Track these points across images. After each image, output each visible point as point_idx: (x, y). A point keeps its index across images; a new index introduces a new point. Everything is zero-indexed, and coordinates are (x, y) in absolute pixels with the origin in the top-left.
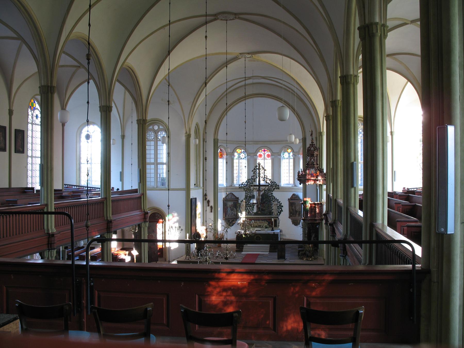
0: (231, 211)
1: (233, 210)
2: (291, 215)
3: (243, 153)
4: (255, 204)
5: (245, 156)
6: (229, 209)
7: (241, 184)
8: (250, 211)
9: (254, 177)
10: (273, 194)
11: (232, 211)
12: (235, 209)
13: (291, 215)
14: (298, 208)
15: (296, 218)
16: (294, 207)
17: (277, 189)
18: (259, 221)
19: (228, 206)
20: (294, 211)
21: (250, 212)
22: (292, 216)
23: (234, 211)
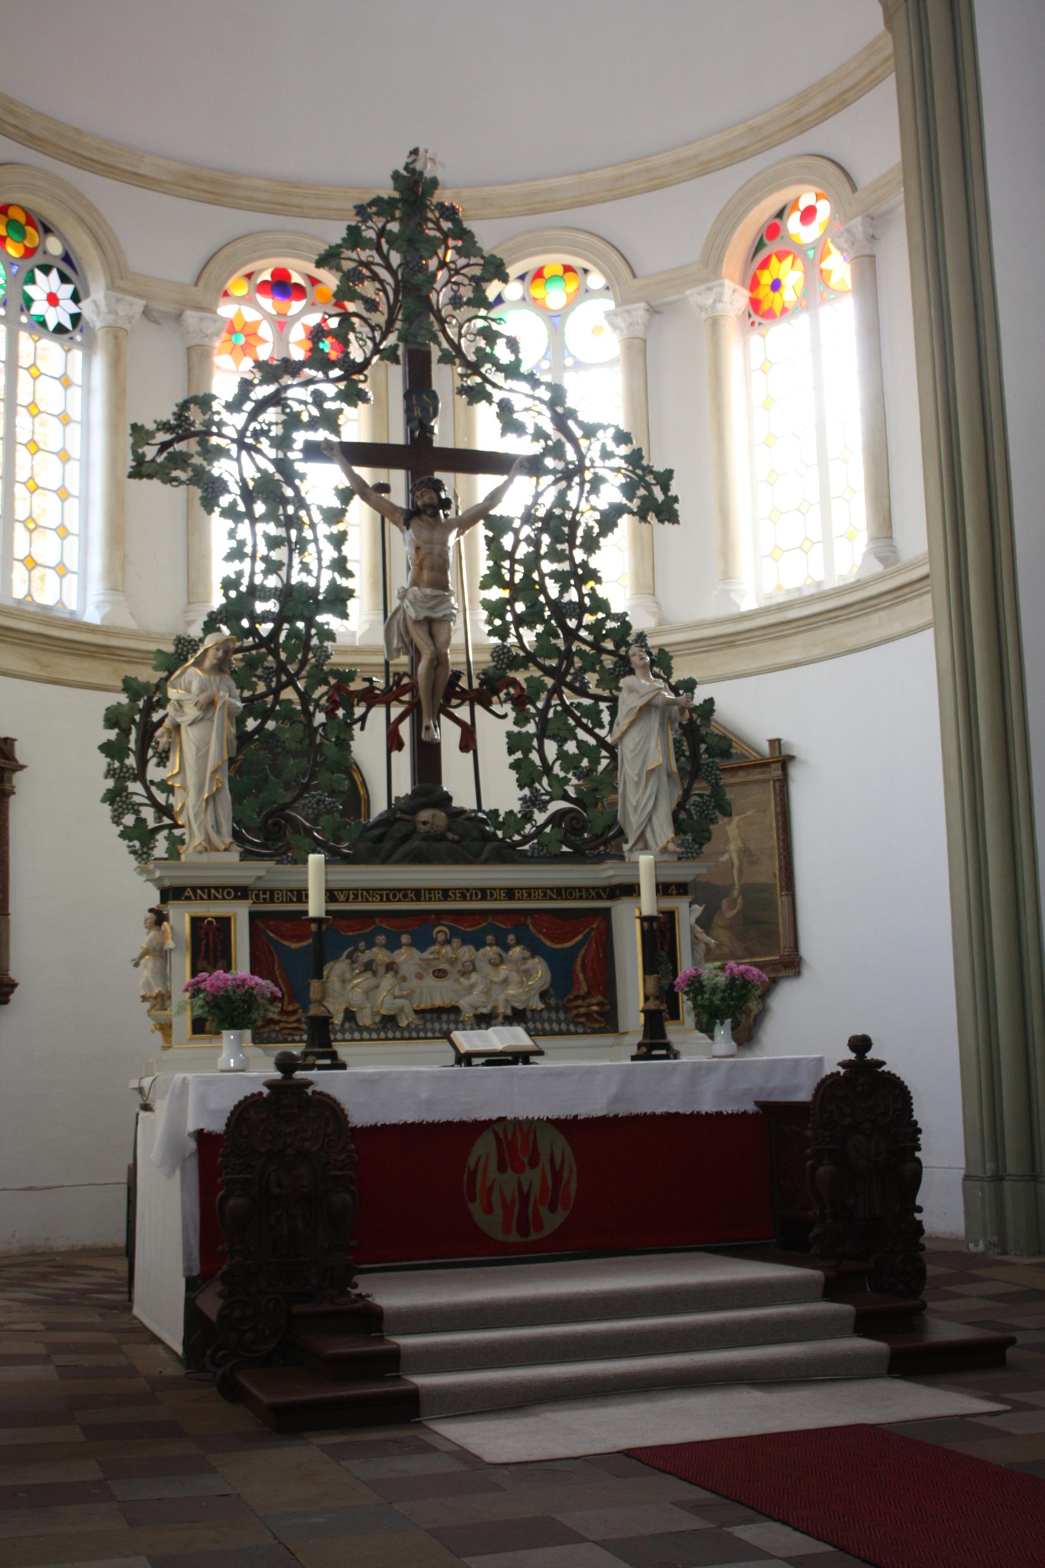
3: (54, 273)
4: (358, 711)
5: (74, 309)
7: (165, 427)
9: (346, 343)
10: (592, 575)
17: (643, 518)
18: (422, 943)
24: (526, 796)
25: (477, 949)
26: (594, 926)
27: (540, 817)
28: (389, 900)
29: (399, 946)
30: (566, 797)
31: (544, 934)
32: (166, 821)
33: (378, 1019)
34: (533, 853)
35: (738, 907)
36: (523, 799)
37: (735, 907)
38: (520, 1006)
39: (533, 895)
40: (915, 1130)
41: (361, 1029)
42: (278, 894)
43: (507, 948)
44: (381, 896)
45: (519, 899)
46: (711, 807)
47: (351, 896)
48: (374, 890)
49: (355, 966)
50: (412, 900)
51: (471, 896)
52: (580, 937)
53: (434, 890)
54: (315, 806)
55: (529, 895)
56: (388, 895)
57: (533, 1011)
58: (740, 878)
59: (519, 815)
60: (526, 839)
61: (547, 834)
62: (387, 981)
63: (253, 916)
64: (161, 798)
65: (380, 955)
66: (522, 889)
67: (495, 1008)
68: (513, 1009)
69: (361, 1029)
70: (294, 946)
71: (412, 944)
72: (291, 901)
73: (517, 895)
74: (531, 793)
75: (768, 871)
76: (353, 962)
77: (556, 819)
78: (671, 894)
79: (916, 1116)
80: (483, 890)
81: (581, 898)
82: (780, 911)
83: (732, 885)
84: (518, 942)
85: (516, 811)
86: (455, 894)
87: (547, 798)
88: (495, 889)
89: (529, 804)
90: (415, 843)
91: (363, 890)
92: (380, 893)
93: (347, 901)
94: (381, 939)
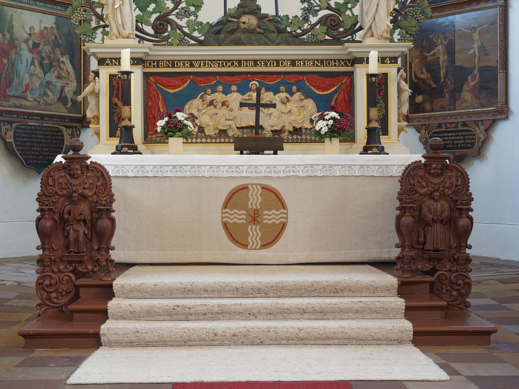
0: (38, 70)
1: (51, 66)
2: (419, 99)
6: (26, 55)
8: (169, 14)
11: (46, 69)
12: (65, 59)
13: (419, 99)
14: (476, 46)
15: (462, 115)
16: (440, 48)
18: (243, 90)
19: (20, 33)
20: (442, 73)
21: (170, 22)
22: (428, 107)
23: (59, 77)
24: (305, 7)
25: (275, 95)
26: (344, 82)
27: (313, 20)
28: (223, 66)
29: (230, 92)
30: (329, 8)
31: (314, 86)
32: (102, 23)
33: (217, 131)
34: (308, 40)
35: (477, 80)
36: (303, 9)
37: (475, 80)
38: (298, 126)
39: (306, 63)
40: (470, 198)
41: (206, 137)
42: (161, 63)
43: (292, 94)
44: (219, 64)
45: (298, 66)
46: (418, 13)
47: (202, 64)
48: (215, 61)
49: (204, 102)
50: (236, 66)
51: (270, 64)
52: (335, 88)
53: (249, 60)
54: (183, 14)
55: (304, 63)
56: (222, 63)
57: (306, 129)
58: (478, 64)
59: (301, 19)
60: (305, 32)
61: (317, 29)
62: (223, 111)
63: (146, 75)
64: (99, 10)
65: (219, 97)
66: (300, 60)
67: (283, 126)
68: (294, 127)
69: (206, 137)
70: (171, 91)
71: (238, 91)
72: (169, 67)
73: (297, 64)
74: (309, 6)
75: (494, 60)
76: (203, 101)
77: (323, 21)
78: (387, 63)
79: (471, 190)
80: (277, 61)
81: (335, 65)
82: (499, 81)
83: (475, 67)
84: (298, 91)
85: (299, 16)
86: (261, 63)
87: (318, 8)
88: (284, 60)
89: (307, 12)
90: (238, 35)
91: (208, 60)
92: (218, 62)
93: (200, 66)
94: (220, 88)
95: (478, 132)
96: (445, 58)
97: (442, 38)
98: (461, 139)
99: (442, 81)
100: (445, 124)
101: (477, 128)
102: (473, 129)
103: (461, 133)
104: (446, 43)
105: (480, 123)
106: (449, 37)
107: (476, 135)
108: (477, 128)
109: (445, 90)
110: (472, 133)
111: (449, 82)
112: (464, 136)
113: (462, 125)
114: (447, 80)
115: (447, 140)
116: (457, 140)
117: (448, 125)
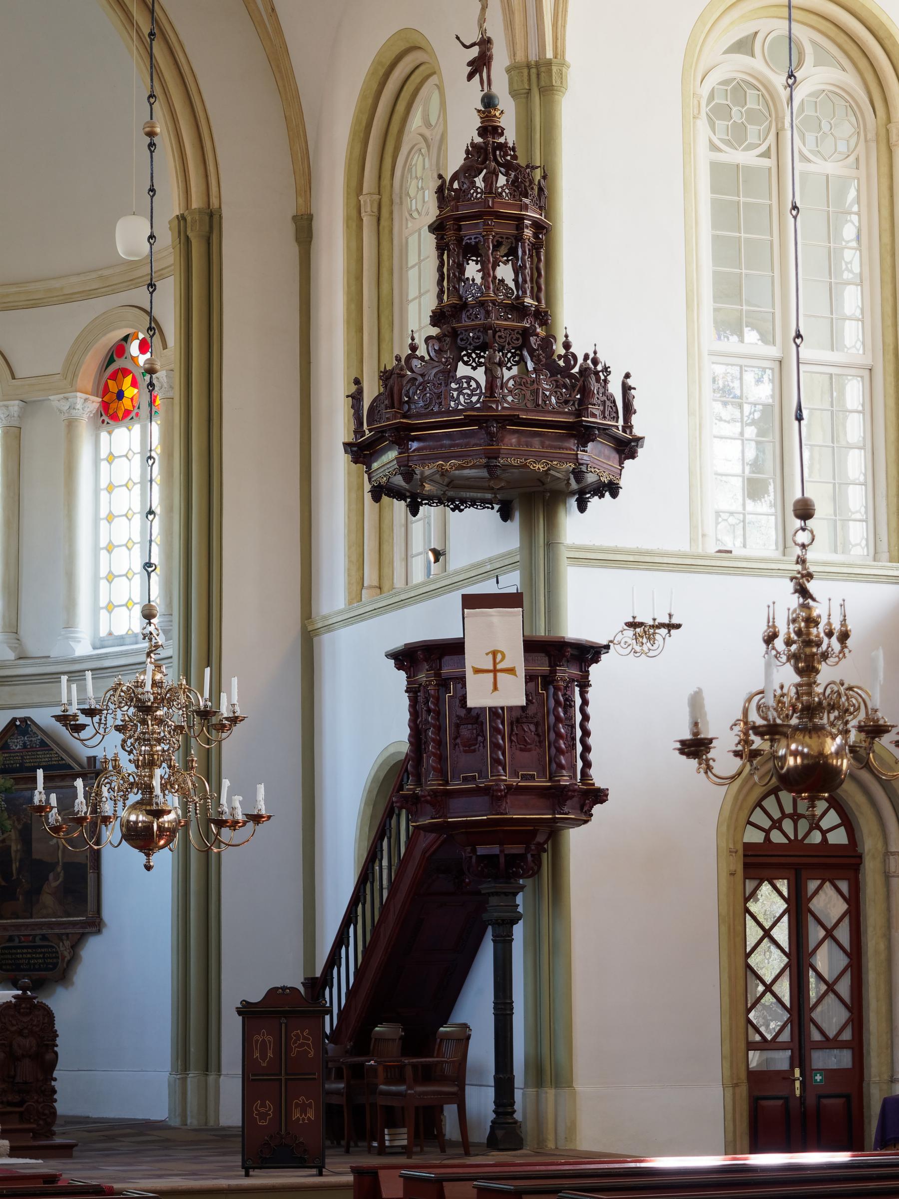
95: (62, 949)
96: (19, 847)
97: (15, 819)
98: (40, 958)
99: (15, 877)
100: (18, 936)
101: (61, 944)
102: (56, 944)
103: (39, 950)
104: (19, 827)
105: (64, 937)
106: (25, 820)
107: (60, 953)
108: (61, 944)
109: (18, 890)
110: (54, 950)
111: (24, 881)
112: (44, 953)
113: (40, 939)
114: (21, 877)
115: (21, 959)
116: (33, 958)
117: (23, 938)
